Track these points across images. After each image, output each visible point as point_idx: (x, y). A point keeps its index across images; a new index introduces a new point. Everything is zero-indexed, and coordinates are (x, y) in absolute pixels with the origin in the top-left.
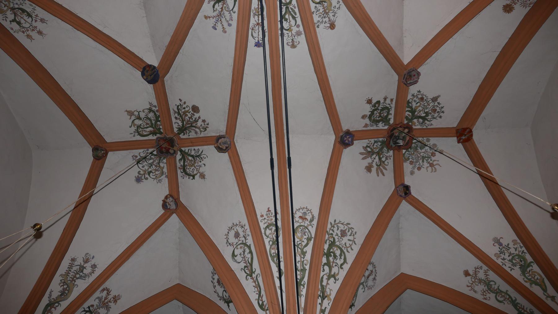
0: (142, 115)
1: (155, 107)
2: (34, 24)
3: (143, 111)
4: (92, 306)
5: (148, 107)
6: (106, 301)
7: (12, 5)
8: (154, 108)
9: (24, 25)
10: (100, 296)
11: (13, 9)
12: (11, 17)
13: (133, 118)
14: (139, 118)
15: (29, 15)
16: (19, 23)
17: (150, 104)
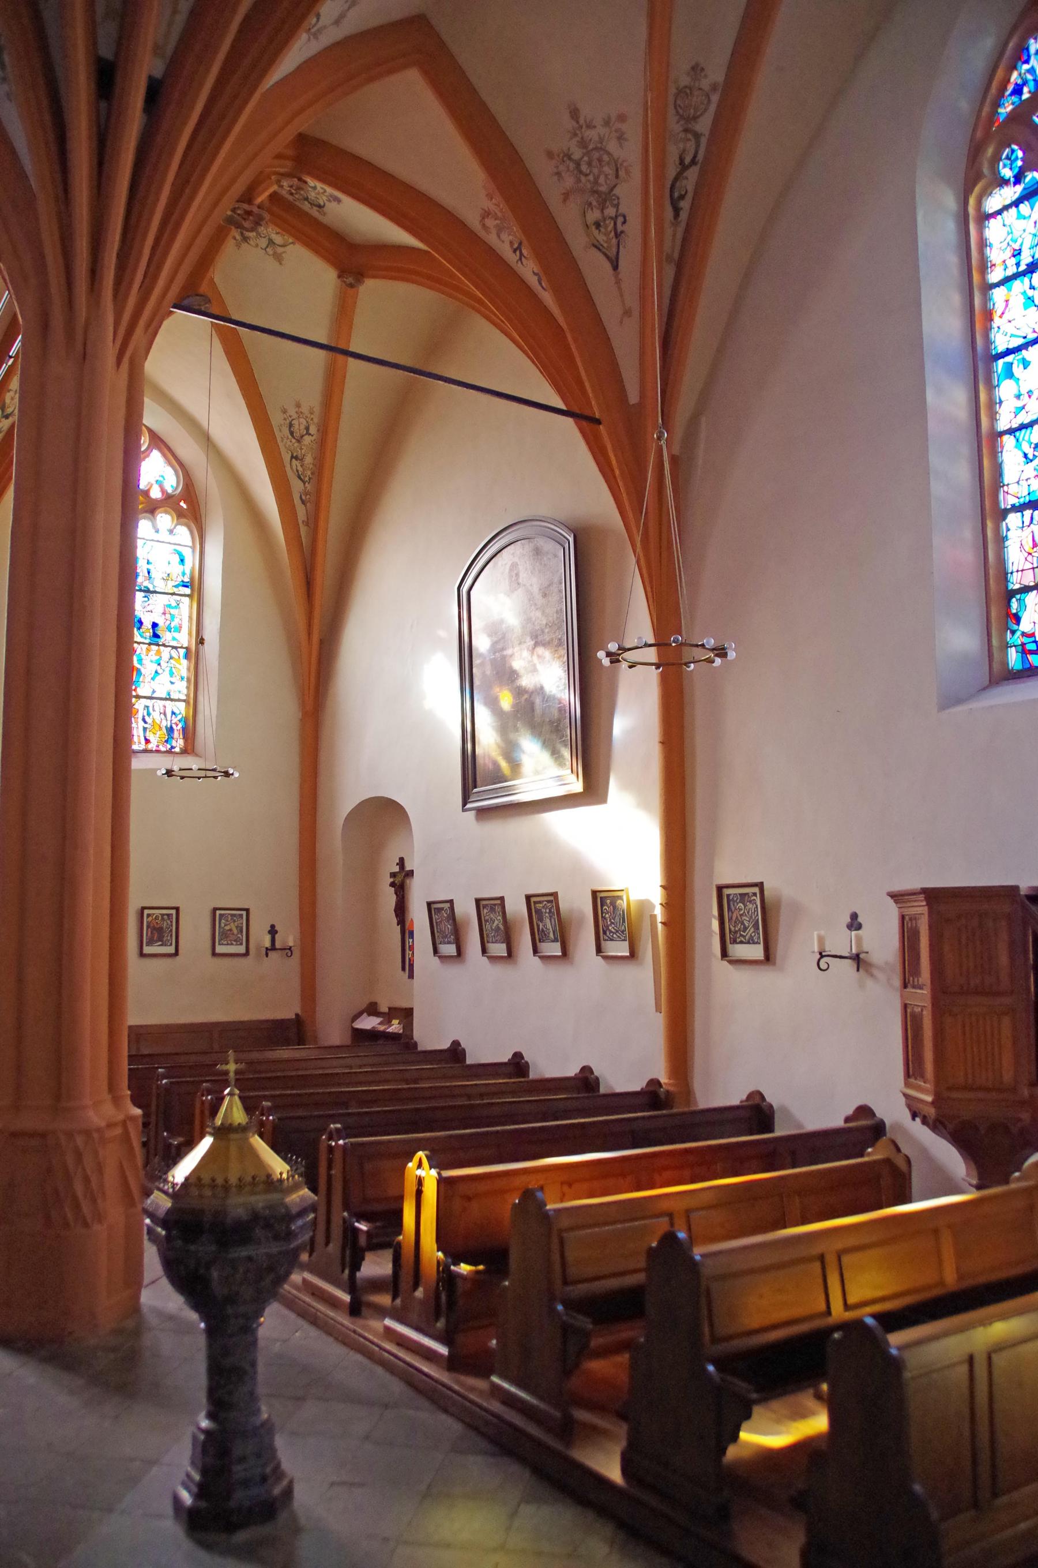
0: (263, 243)
1: (235, 238)
2: (295, 416)
3: (257, 245)
4: (511, 243)
5: (244, 245)
6: (499, 214)
7: (296, 445)
8: (238, 237)
9: (305, 423)
10: (494, 231)
11: (298, 441)
12: (307, 439)
13: (280, 250)
14: (271, 242)
15: (291, 425)
16: (307, 428)
17: (238, 246)
